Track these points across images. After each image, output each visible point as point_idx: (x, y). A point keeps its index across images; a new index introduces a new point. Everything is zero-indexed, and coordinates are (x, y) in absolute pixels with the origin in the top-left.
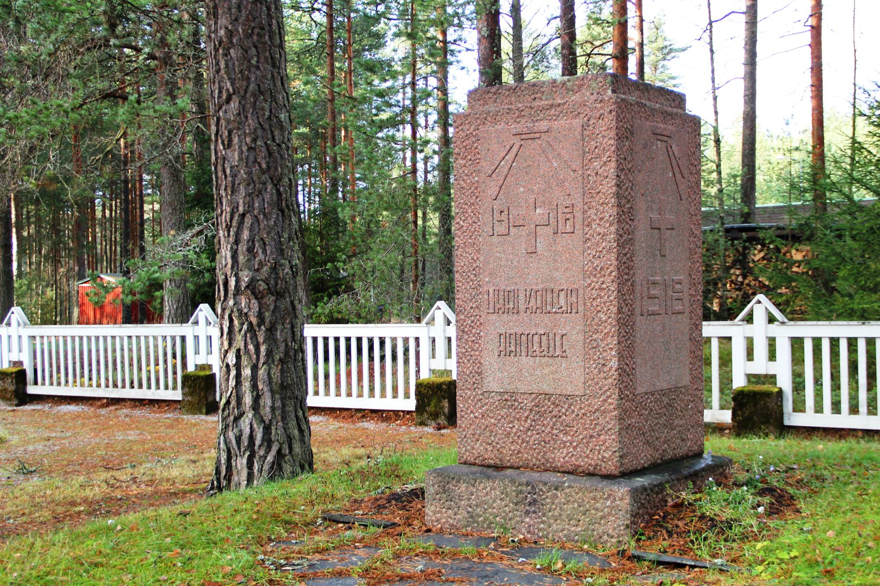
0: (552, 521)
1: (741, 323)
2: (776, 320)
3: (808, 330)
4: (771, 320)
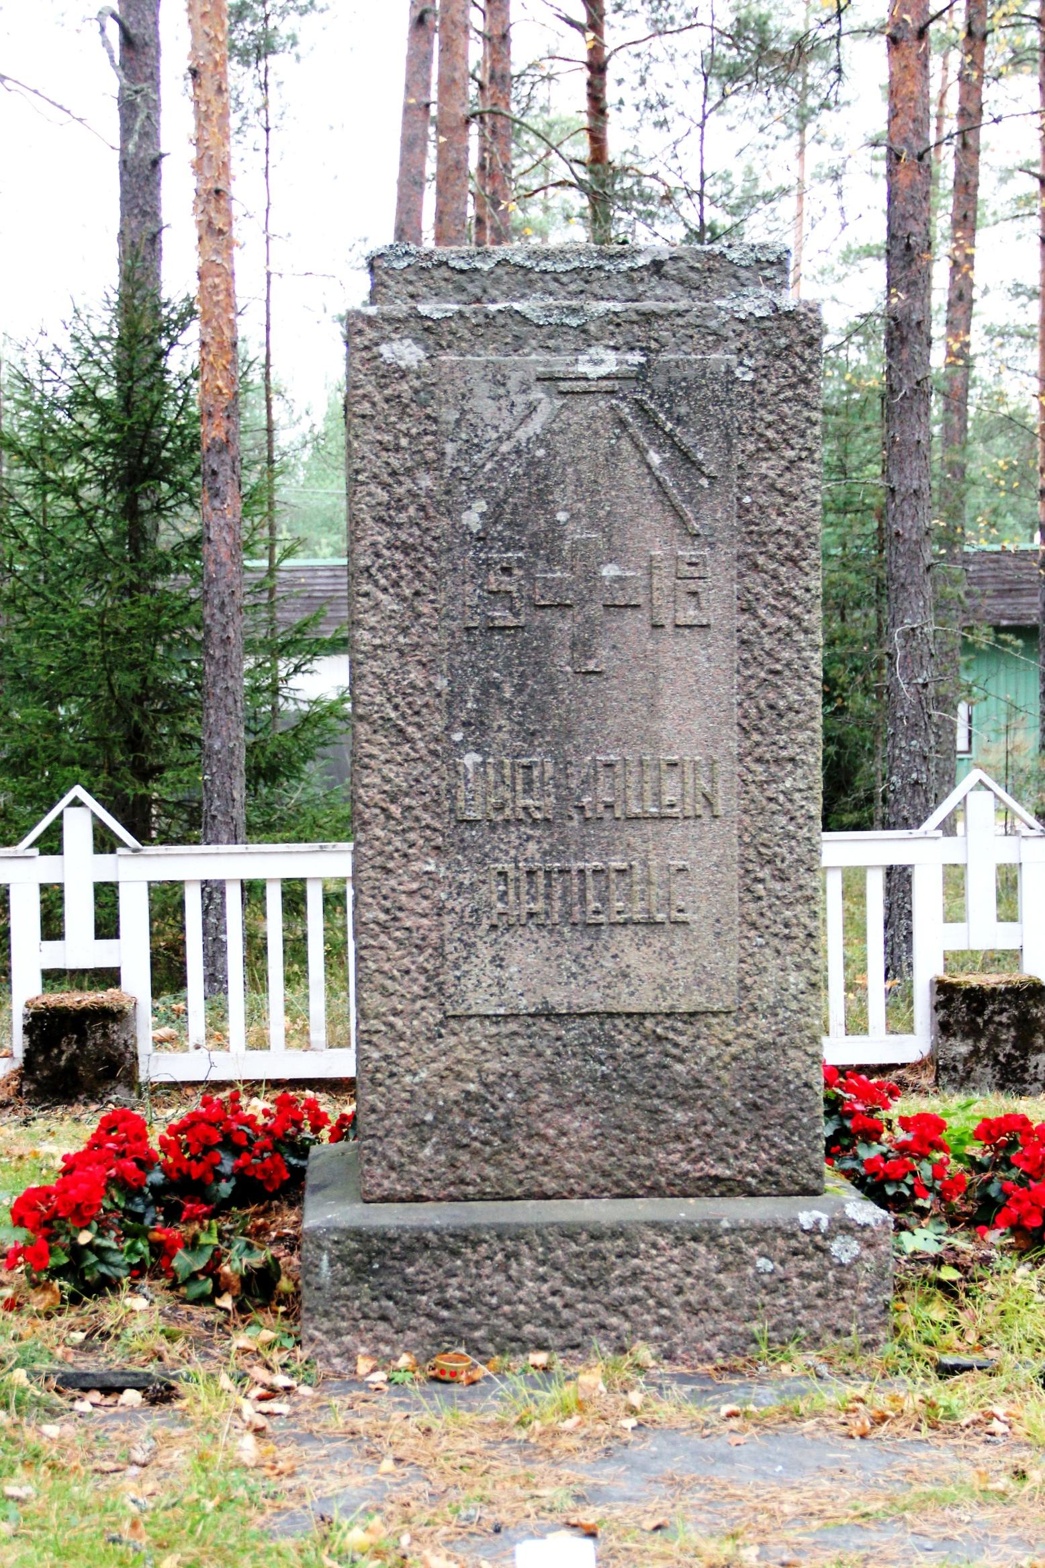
0: (683, 1316)
1: (35, 851)
2: (125, 845)
3: (188, 865)
4: (104, 842)
